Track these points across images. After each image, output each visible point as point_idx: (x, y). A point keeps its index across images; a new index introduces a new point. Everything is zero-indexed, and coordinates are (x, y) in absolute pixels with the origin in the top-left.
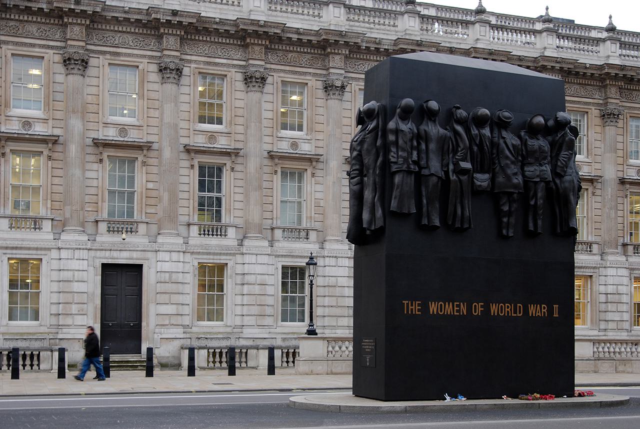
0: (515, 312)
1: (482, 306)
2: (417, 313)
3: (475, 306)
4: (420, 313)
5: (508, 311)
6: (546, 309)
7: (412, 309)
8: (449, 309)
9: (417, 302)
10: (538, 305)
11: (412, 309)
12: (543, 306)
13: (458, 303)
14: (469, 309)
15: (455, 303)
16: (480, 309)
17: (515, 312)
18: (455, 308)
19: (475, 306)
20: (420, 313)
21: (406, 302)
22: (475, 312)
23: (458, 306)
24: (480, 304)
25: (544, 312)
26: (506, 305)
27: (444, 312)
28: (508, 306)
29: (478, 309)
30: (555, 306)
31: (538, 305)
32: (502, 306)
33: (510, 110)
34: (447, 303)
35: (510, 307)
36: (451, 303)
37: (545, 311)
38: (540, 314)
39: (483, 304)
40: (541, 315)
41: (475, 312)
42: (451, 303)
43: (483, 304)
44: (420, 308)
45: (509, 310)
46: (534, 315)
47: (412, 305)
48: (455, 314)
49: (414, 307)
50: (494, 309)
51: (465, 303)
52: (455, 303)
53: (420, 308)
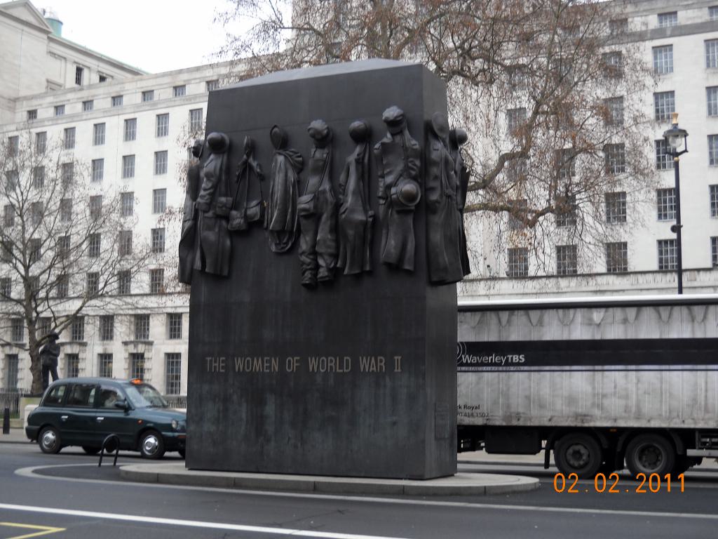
0: (341, 367)
1: (297, 361)
2: (221, 371)
3: (290, 361)
4: (223, 371)
5: (331, 367)
6: (384, 362)
7: (215, 367)
8: (257, 365)
9: (221, 359)
10: (373, 359)
11: (215, 367)
12: (379, 358)
13: (268, 358)
14: (282, 364)
15: (265, 358)
16: (295, 365)
17: (341, 367)
18: (265, 365)
19: (290, 361)
20: (223, 371)
21: (209, 359)
22: (289, 368)
23: (270, 361)
24: (295, 358)
25: (381, 367)
26: (329, 358)
27: (252, 368)
28: (331, 361)
29: (293, 363)
30: (396, 358)
31: (373, 359)
32: (323, 361)
33: (358, 118)
34: (255, 359)
35: (333, 359)
36: (260, 360)
37: (383, 364)
38: (375, 369)
39: (298, 358)
40: (377, 368)
41: (289, 368)
42: (260, 360)
43: (298, 358)
44: (224, 365)
45: (333, 364)
46: (367, 370)
47: (215, 362)
48: (265, 370)
49: (217, 365)
50: (313, 363)
51: (277, 359)
52: (265, 358)
53: (224, 365)
